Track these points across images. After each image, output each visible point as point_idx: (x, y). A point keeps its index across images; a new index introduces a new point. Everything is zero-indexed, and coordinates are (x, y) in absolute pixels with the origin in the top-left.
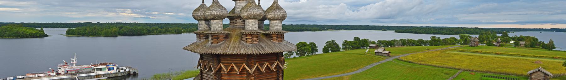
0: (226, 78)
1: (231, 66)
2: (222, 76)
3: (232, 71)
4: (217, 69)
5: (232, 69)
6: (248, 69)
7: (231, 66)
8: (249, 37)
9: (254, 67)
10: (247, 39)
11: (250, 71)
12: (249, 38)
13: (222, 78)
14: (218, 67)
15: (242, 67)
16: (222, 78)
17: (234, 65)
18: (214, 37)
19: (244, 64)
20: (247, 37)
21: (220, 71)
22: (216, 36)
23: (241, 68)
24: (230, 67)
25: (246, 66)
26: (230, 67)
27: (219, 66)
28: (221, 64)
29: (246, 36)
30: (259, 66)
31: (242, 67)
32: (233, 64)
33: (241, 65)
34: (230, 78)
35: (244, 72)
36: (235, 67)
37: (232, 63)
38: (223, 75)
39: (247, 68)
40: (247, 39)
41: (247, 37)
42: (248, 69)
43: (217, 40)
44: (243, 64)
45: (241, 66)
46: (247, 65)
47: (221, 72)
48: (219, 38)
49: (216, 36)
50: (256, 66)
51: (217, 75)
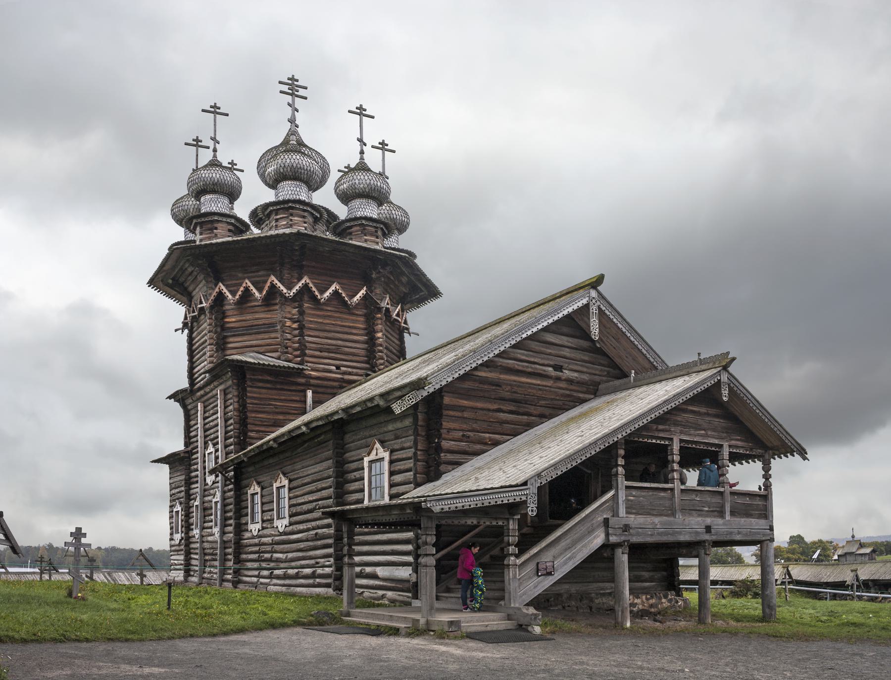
0: (234, 320)
3: (245, 303)
5: (247, 295)
6: (282, 288)
8: (281, 216)
10: (277, 220)
11: (285, 291)
12: (283, 218)
13: (226, 320)
15: (268, 284)
16: (226, 320)
19: (273, 278)
20: (278, 217)
21: (222, 305)
23: (266, 288)
25: (276, 281)
31: (268, 284)
33: (265, 278)
34: (244, 318)
35: (275, 299)
36: (252, 287)
39: (279, 284)
42: (282, 288)
44: (269, 276)
45: (266, 282)
47: (224, 308)
50: (303, 281)
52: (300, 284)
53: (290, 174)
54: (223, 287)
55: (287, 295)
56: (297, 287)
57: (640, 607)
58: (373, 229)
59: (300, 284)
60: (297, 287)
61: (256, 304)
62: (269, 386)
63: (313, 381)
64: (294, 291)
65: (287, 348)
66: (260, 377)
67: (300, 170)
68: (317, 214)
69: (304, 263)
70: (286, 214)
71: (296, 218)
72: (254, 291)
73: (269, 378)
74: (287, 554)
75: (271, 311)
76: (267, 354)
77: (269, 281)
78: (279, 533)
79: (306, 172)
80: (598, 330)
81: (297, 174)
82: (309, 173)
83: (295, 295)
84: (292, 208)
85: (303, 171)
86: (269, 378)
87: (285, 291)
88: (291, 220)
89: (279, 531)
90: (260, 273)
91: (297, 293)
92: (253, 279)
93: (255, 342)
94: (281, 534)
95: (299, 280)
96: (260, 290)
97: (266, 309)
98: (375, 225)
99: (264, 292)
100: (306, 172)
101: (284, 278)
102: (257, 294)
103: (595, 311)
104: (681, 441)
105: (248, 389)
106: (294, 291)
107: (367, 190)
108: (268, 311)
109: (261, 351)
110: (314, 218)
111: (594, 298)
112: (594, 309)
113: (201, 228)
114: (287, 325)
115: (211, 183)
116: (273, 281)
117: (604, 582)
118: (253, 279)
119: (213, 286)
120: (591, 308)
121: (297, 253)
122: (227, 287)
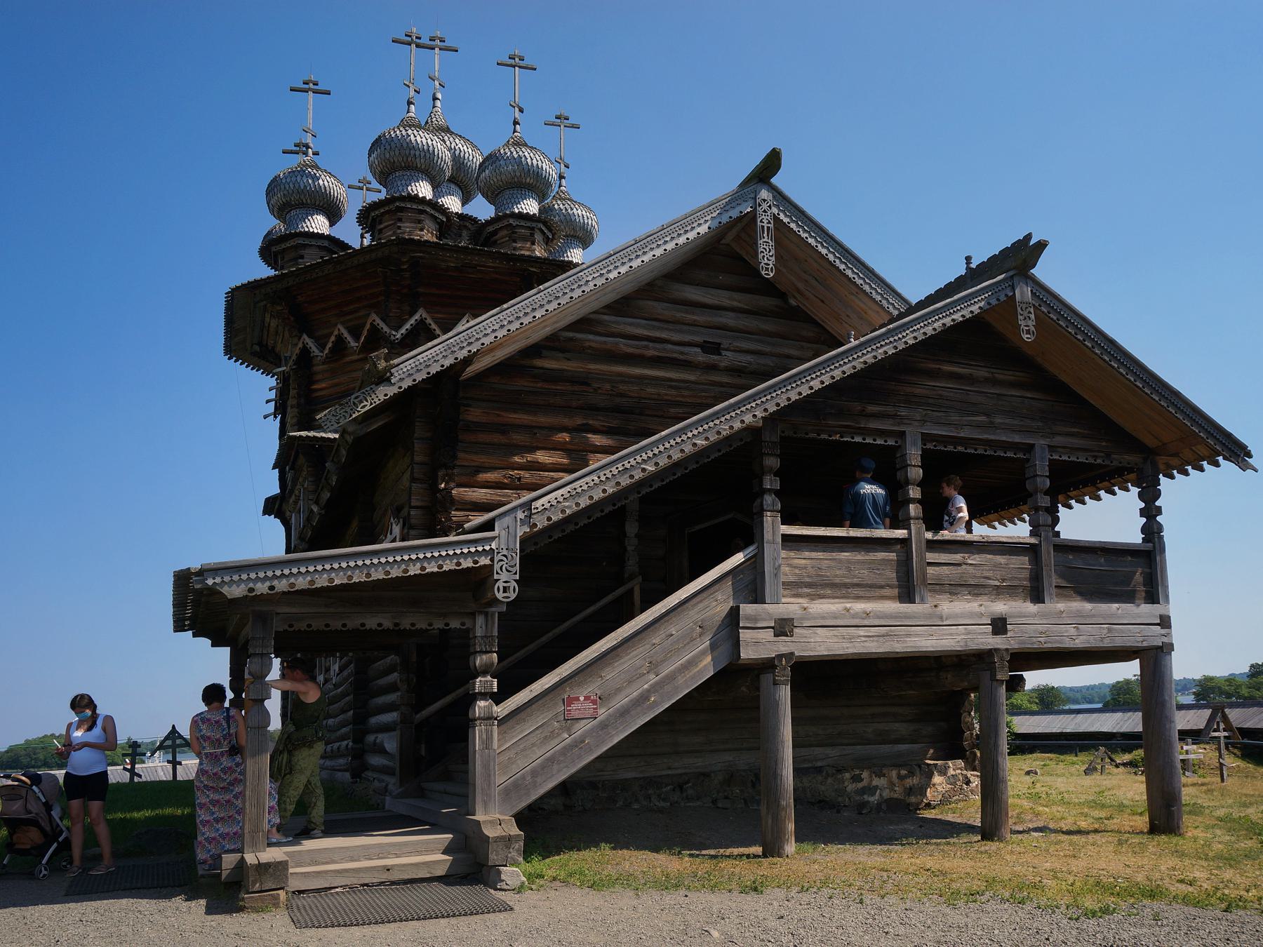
0: (324, 385)
1: (336, 333)
6: (386, 329)
7: (336, 333)
8: (386, 224)
14: (297, 351)
15: (368, 326)
19: (374, 316)
20: (382, 226)
23: (365, 333)
24: (333, 338)
25: (378, 321)
26: (333, 338)
30: (429, 321)
31: (368, 326)
32: (340, 327)
37: (336, 325)
41: (382, 226)
42: (386, 329)
44: (368, 315)
46: (383, 320)
50: (417, 317)
52: (412, 321)
55: (392, 337)
56: (408, 326)
57: (886, 794)
58: (527, 232)
59: (412, 321)
60: (408, 326)
61: (355, 357)
64: (403, 331)
67: (412, 152)
68: (441, 217)
69: (419, 290)
71: (408, 225)
72: (349, 339)
77: (369, 321)
79: (423, 154)
80: (773, 259)
81: (409, 159)
82: (428, 155)
83: (405, 337)
85: (417, 153)
88: (399, 228)
91: (406, 334)
95: (411, 314)
96: (357, 338)
98: (529, 224)
100: (423, 154)
101: (391, 315)
102: (353, 344)
103: (766, 225)
104: (926, 438)
106: (403, 331)
107: (518, 174)
110: (438, 223)
111: (764, 200)
112: (764, 221)
115: (295, 191)
116: (374, 321)
117: (811, 746)
120: (759, 221)
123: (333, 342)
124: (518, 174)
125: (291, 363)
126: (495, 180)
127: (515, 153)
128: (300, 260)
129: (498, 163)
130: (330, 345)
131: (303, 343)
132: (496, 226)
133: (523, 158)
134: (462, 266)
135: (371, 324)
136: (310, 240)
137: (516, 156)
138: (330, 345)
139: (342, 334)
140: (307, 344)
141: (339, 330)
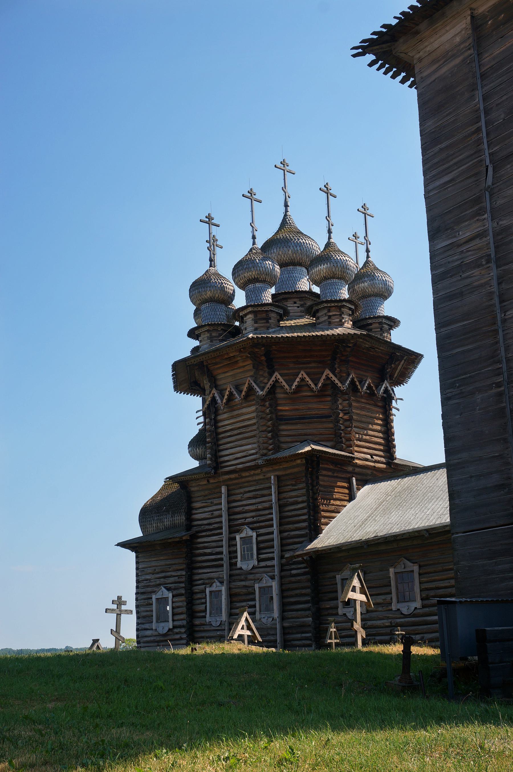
0: (287, 408)
2: (278, 405)
4: (268, 386)
6: (337, 381)
7: (300, 376)
8: (334, 313)
9: (347, 379)
10: (330, 317)
11: (340, 385)
13: (279, 408)
14: (271, 382)
15: (324, 377)
16: (279, 408)
17: (305, 376)
18: (259, 316)
19: (327, 372)
22: (264, 315)
24: (298, 380)
25: (331, 375)
26: (298, 380)
27: (273, 378)
28: (276, 374)
29: (329, 311)
30: (355, 380)
31: (324, 377)
32: (302, 372)
34: (297, 407)
38: (280, 402)
39: (334, 378)
40: (330, 317)
41: (331, 314)
42: (337, 381)
43: (268, 322)
48: (270, 319)
49: (264, 315)
51: (267, 404)
53: (340, 274)
54: (279, 377)
62: (330, 473)
63: (357, 470)
65: (341, 438)
66: (326, 466)
70: (338, 312)
73: (331, 467)
74: (422, 635)
75: (323, 401)
76: (320, 443)
78: (402, 616)
84: (344, 306)
86: (331, 467)
87: (340, 385)
89: (402, 614)
90: (310, 365)
92: (308, 370)
93: (309, 431)
94: (406, 616)
97: (319, 400)
99: (320, 385)
105: (320, 477)
108: (320, 402)
109: (315, 439)
113: (256, 316)
114: (340, 416)
116: (328, 374)
118: (308, 370)
119: (266, 374)
121: (349, 349)
122: (281, 375)
123: (298, 382)
124: (383, 290)
125: (266, 389)
126: (370, 290)
127: (383, 277)
128: (270, 321)
129: (374, 281)
130: (296, 383)
131: (276, 378)
132: (374, 321)
133: (387, 282)
134: (370, 347)
135: (326, 376)
136: (277, 309)
137: (384, 279)
138: (296, 383)
139: (305, 378)
140: (279, 379)
141: (302, 375)
